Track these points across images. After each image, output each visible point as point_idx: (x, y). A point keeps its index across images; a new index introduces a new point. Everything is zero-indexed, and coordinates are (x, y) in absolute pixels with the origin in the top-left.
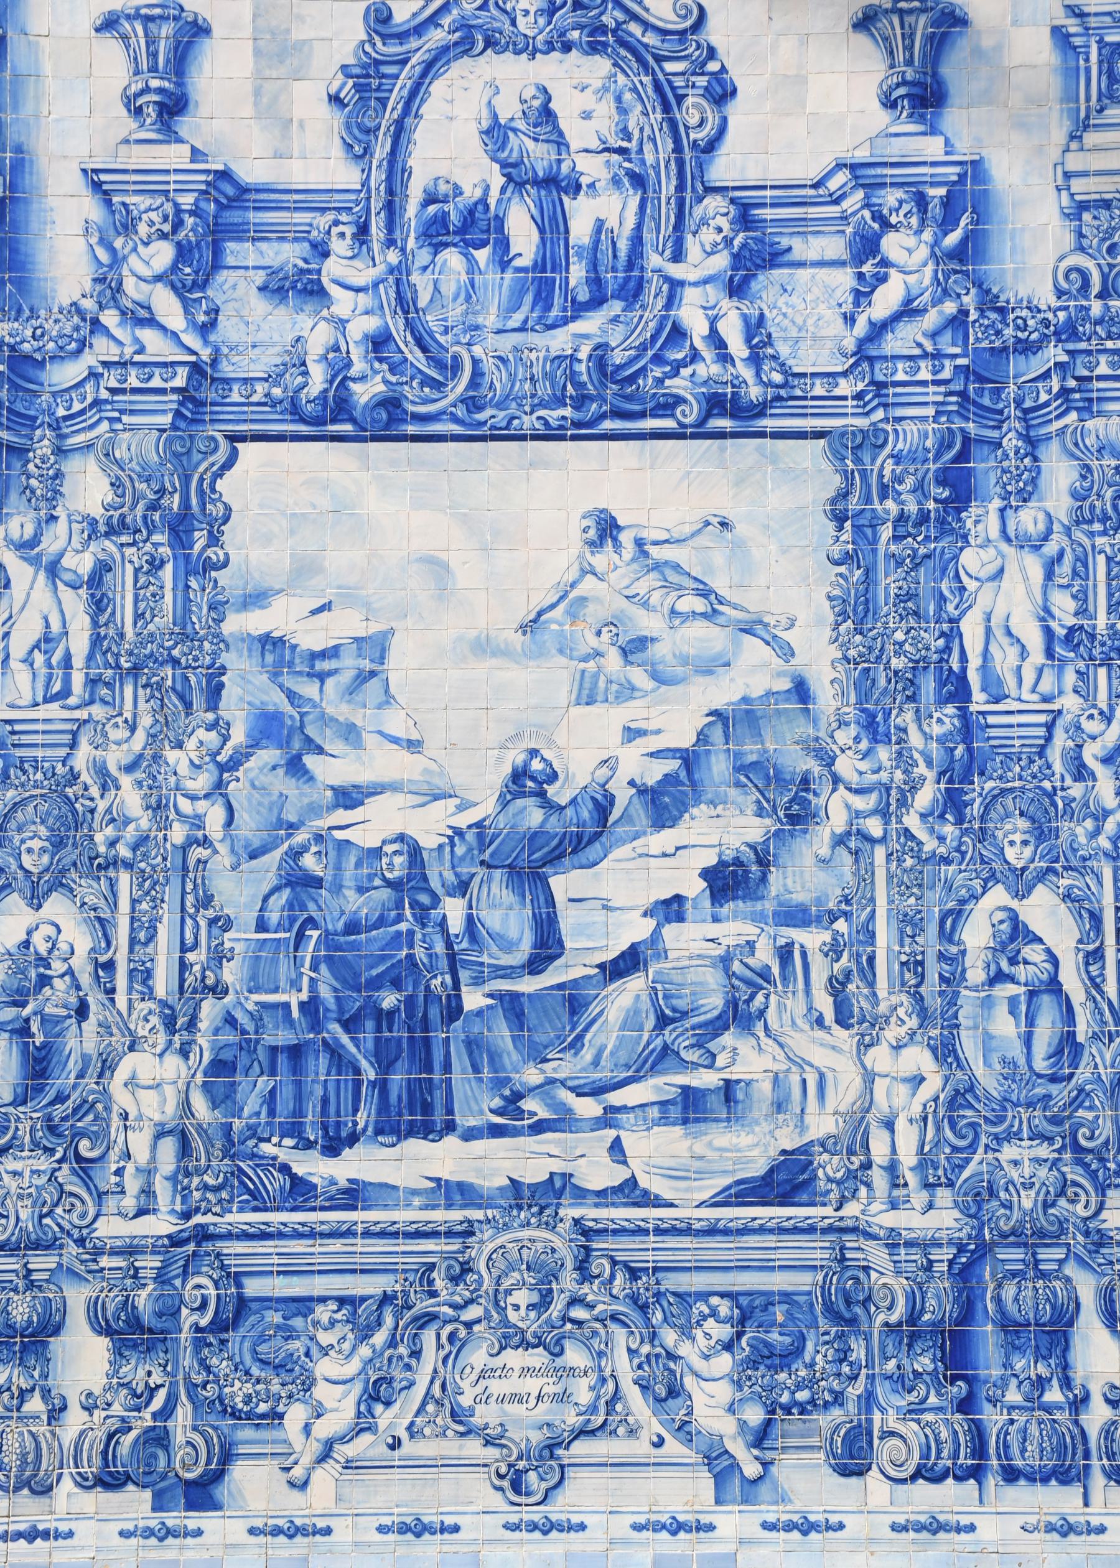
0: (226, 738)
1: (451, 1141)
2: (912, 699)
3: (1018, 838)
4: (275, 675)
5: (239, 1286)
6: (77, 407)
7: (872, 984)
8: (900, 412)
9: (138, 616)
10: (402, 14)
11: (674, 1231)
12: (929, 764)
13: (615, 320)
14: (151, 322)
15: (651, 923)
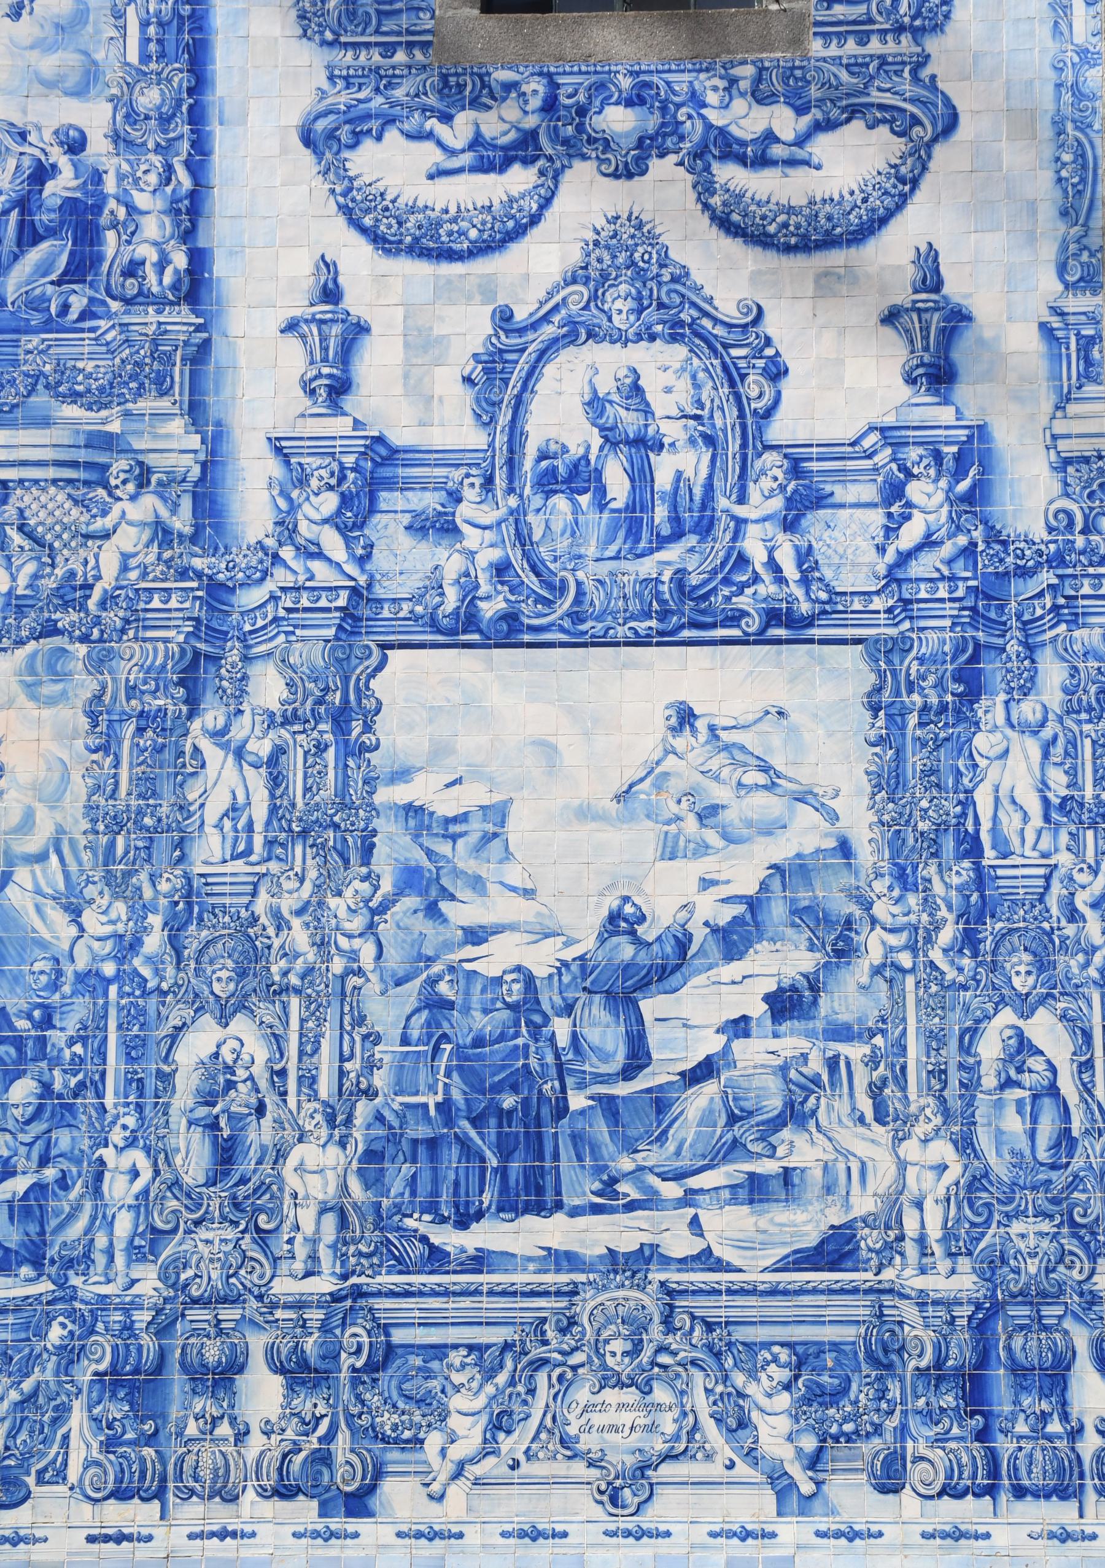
0: (376, 888)
1: (559, 1217)
2: (935, 855)
3: (1023, 969)
4: (416, 837)
5: (387, 1334)
6: (260, 623)
7: (904, 1089)
8: (923, 623)
9: (307, 790)
10: (521, 314)
11: (743, 1292)
12: (950, 908)
13: (691, 550)
14: (320, 555)
15: (722, 1039)
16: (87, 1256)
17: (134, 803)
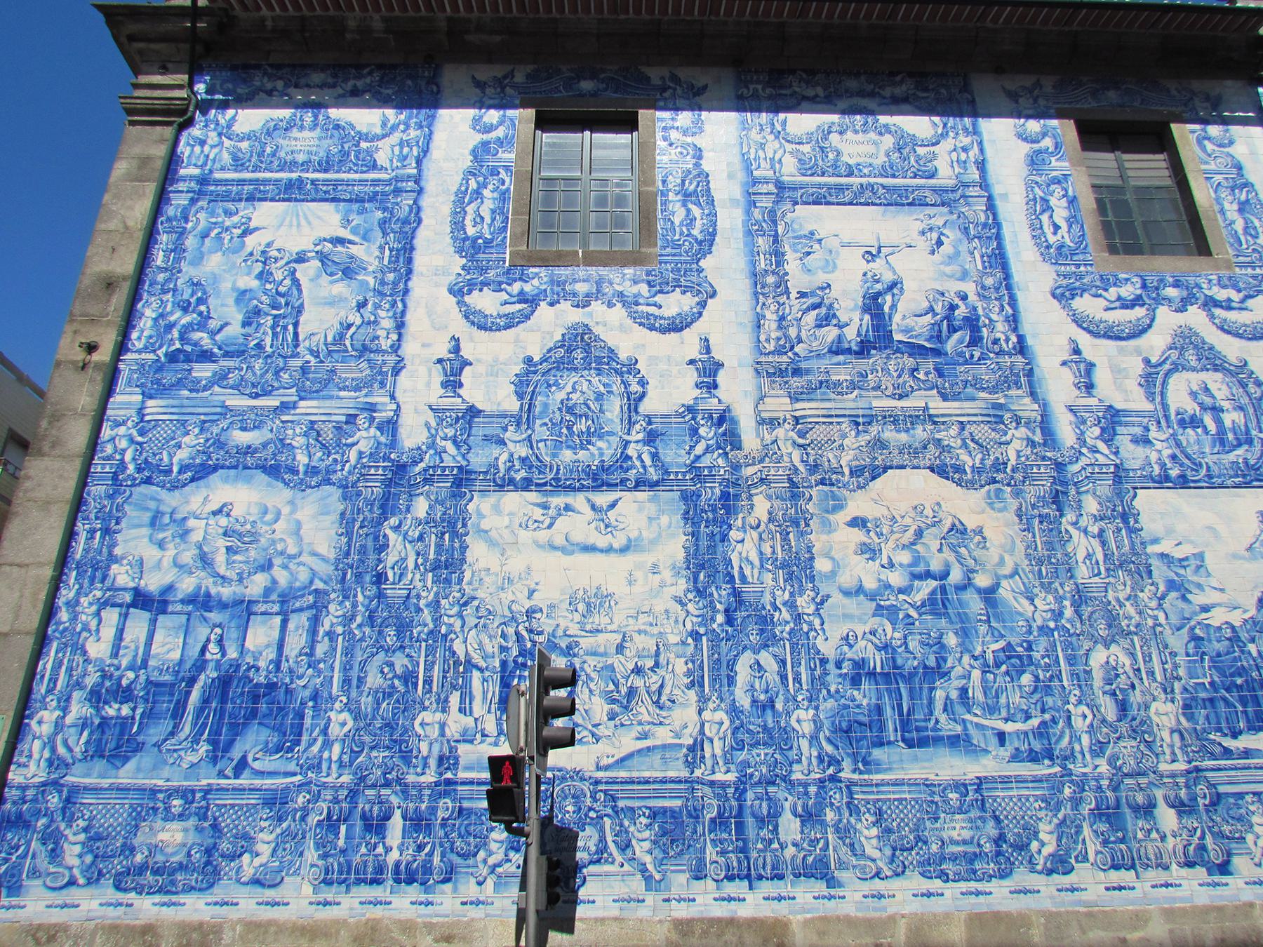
10: (1154, 360)
14: (1098, 452)
16: (1072, 754)
17: (1046, 553)
